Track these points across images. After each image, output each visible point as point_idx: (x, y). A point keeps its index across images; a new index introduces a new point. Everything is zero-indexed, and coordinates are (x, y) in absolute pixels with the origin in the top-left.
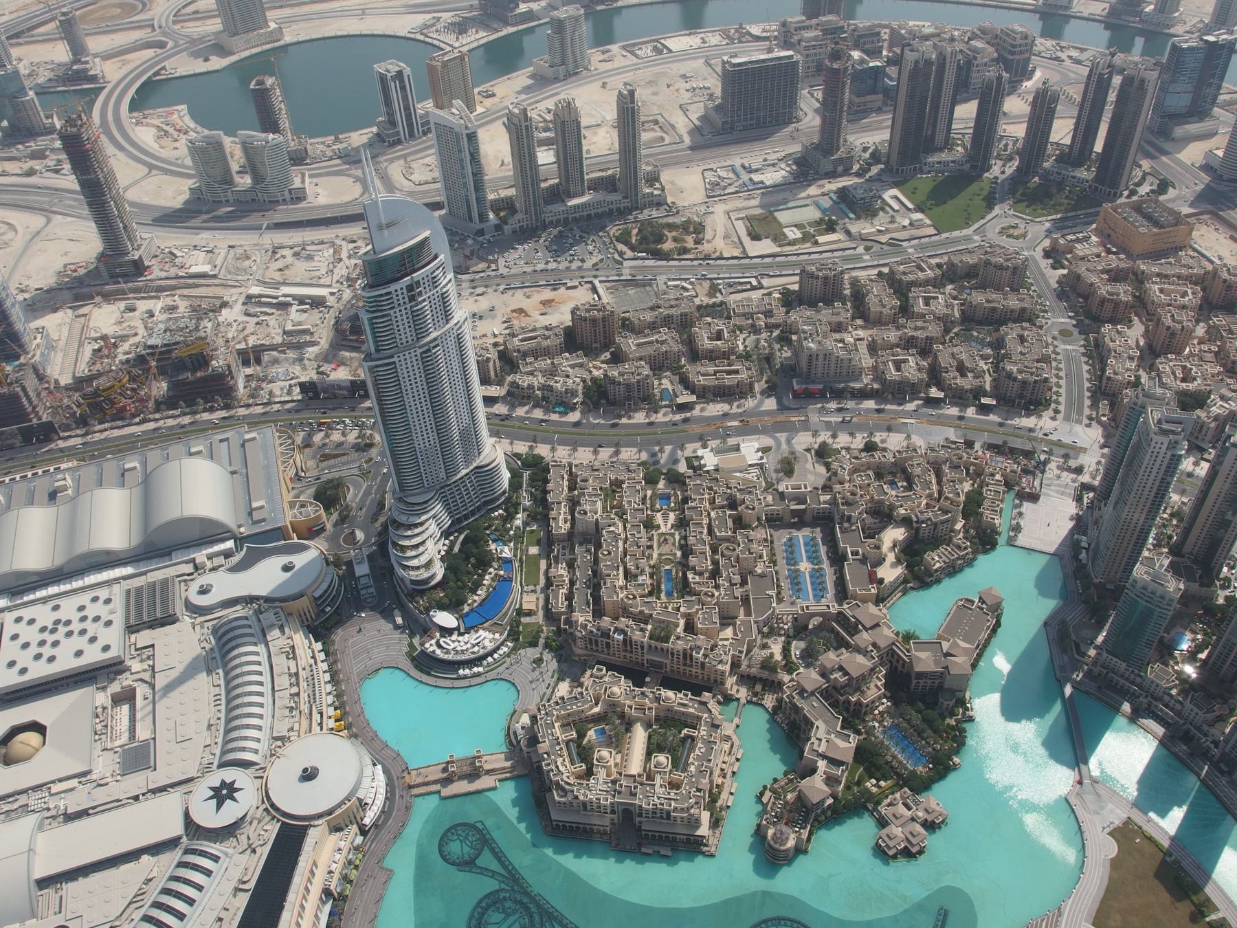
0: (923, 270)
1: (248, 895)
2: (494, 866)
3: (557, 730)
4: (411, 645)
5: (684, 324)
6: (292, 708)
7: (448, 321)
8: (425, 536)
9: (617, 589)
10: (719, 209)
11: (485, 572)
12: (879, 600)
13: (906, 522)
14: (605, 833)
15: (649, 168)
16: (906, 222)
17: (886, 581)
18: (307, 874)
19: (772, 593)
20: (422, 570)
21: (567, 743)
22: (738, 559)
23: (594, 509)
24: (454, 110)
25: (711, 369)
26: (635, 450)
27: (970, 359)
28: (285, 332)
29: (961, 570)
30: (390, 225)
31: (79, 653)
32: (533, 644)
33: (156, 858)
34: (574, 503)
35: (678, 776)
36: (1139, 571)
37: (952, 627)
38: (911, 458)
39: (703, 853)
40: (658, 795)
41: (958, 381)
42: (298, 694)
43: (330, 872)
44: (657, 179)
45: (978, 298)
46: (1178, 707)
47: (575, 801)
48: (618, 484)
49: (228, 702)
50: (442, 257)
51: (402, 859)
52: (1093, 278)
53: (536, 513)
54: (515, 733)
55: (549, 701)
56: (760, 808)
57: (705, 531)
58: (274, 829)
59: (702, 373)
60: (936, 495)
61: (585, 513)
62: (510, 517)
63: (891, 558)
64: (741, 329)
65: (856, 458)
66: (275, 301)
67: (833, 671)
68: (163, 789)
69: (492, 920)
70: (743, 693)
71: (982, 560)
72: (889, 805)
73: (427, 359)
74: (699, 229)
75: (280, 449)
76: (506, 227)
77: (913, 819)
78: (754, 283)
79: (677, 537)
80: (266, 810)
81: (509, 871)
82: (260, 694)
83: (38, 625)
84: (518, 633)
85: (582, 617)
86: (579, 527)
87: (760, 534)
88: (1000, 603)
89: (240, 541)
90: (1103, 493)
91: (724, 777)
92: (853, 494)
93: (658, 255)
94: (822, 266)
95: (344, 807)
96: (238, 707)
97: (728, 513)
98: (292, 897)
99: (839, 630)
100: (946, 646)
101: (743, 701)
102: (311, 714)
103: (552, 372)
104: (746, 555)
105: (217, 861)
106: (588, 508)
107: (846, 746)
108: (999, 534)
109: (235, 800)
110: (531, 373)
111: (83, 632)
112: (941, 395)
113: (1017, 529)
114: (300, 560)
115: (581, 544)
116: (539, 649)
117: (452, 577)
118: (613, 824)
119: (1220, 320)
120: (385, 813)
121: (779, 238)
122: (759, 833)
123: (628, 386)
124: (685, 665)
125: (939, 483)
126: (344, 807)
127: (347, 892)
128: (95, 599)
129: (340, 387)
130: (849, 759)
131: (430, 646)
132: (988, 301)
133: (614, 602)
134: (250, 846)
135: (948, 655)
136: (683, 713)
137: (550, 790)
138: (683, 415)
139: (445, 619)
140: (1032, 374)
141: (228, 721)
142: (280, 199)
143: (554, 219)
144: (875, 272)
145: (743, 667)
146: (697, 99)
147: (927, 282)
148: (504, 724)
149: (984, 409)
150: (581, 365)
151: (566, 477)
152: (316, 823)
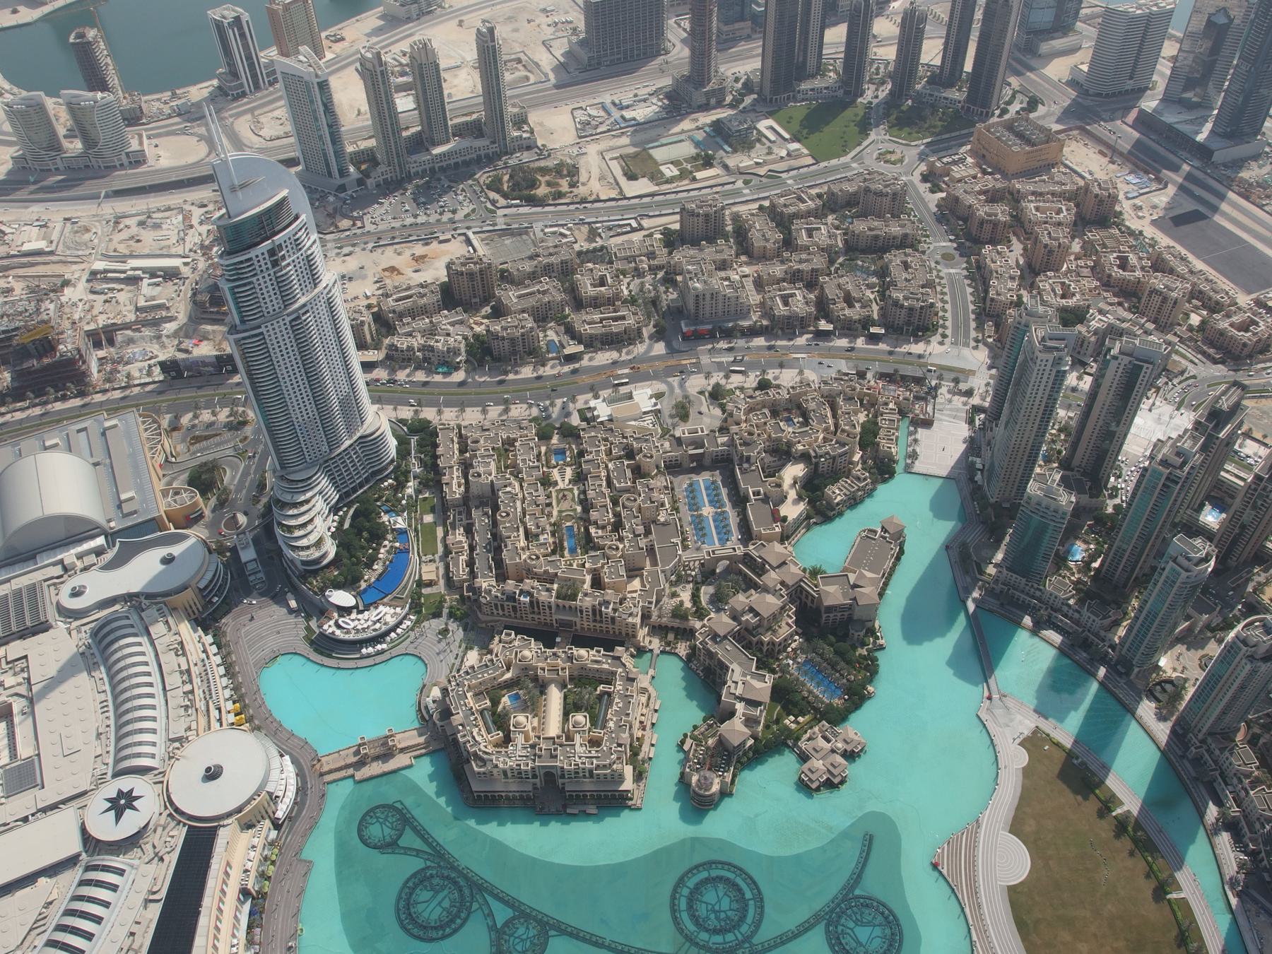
0: (804, 202)
1: (159, 906)
2: (418, 844)
3: (470, 701)
4: (308, 628)
5: (565, 272)
6: (187, 706)
7: (316, 285)
8: (312, 514)
9: (518, 550)
10: (592, 149)
11: (380, 545)
12: (784, 538)
13: (805, 457)
14: (529, 798)
15: (516, 110)
16: (784, 153)
17: (790, 519)
18: (221, 875)
20: (312, 550)
21: (482, 712)
22: (640, 510)
23: (488, 470)
24: (301, 58)
25: (597, 317)
26: (525, 406)
27: (855, 288)
28: (137, 309)
29: (862, 501)
30: (243, 186)
32: (437, 615)
33: (54, 880)
34: (466, 466)
35: (597, 733)
36: (1033, 488)
37: (857, 559)
38: (805, 393)
39: (629, 807)
40: (579, 755)
41: (847, 312)
42: (192, 692)
43: (246, 871)
44: (525, 121)
45: (860, 226)
46: (1076, 615)
47: (495, 771)
48: (510, 442)
49: (116, 707)
50: (303, 217)
51: (322, 849)
52: (970, 200)
53: (428, 480)
54: (426, 707)
55: (458, 671)
56: (681, 756)
57: (604, 483)
58: (180, 834)
59: (588, 322)
60: (832, 428)
61: (479, 475)
62: (400, 486)
63: (792, 494)
64: (624, 273)
65: (751, 397)
66: (123, 276)
67: (743, 613)
68: (55, 806)
69: (421, 899)
70: (656, 644)
71: (881, 488)
72: (809, 739)
73: (297, 326)
74: (573, 171)
75: (145, 435)
76: (369, 181)
77: (833, 751)
78: (634, 224)
79: (576, 492)
80: (170, 815)
81: (433, 848)
82: (151, 696)
84: (421, 605)
85: (486, 582)
86: (474, 490)
87: (659, 482)
88: (902, 531)
89: (111, 536)
90: (994, 414)
91: (644, 729)
92: (751, 434)
93: (532, 201)
94: (702, 203)
95: (254, 803)
96: (128, 711)
98: (209, 901)
99: (746, 573)
100: (852, 578)
101: (657, 651)
102: (208, 710)
103: (431, 332)
104: (648, 504)
105: (122, 875)
106: (481, 470)
107: (762, 687)
108: (896, 462)
109: (134, 809)
110: (410, 334)
112: (830, 327)
113: (914, 456)
114: (176, 550)
115: (477, 507)
116: (444, 619)
117: (345, 553)
118: (535, 788)
119: (1093, 235)
120: (299, 803)
121: (656, 177)
122: (683, 780)
123: (513, 341)
124: (595, 621)
125: (834, 416)
126: (254, 803)
127: (266, 890)
129: (205, 364)
130: (766, 698)
131: (329, 627)
132: (870, 229)
133: (516, 564)
134: (156, 854)
135: (855, 586)
137: (468, 761)
138: (572, 367)
139: (342, 598)
140: (918, 300)
141: (119, 727)
142: (117, 164)
143: (420, 169)
144: (756, 205)
145: (654, 617)
146: (560, 34)
147: (809, 213)
148: (414, 699)
149: (874, 339)
150: (461, 322)
151: (456, 439)
152: (226, 822)
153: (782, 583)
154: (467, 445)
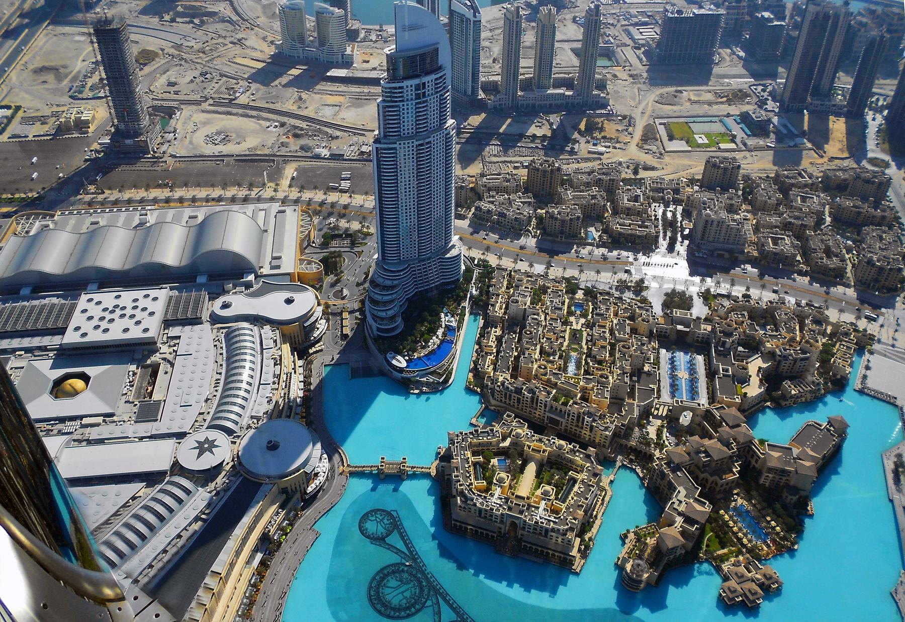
2: (400, 545)
8: (394, 296)
19: (655, 387)
21: (475, 464)
22: (631, 356)
31: (126, 330)
47: (473, 508)
48: (544, 290)
49: (226, 384)
85: (503, 377)
97: (628, 322)
98: (239, 531)
105: (188, 495)
106: (520, 299)
109: (212, 452)
111: (132, 316)
124: (577, 426)
125: (801, 330)
128: (147, 296)
136: (570, 461)
137: (455, 497)
141: (222, 397)
153: (735, 440)
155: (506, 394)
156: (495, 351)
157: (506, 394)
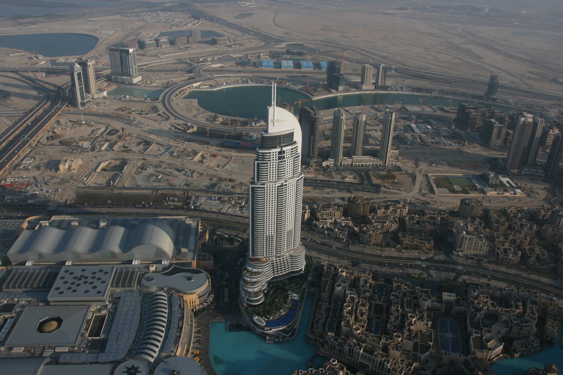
79: (385, 307)
83: (73, 276)
111: (92, 283)
124: (379, 369)
128: (101, 271)
154: (338, 272)
155: (332, 346)
156: (324, 316)
157: (332, 346)
